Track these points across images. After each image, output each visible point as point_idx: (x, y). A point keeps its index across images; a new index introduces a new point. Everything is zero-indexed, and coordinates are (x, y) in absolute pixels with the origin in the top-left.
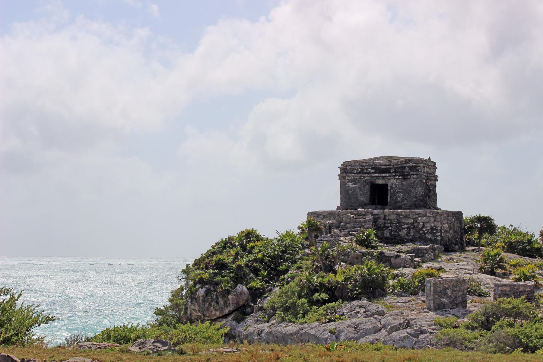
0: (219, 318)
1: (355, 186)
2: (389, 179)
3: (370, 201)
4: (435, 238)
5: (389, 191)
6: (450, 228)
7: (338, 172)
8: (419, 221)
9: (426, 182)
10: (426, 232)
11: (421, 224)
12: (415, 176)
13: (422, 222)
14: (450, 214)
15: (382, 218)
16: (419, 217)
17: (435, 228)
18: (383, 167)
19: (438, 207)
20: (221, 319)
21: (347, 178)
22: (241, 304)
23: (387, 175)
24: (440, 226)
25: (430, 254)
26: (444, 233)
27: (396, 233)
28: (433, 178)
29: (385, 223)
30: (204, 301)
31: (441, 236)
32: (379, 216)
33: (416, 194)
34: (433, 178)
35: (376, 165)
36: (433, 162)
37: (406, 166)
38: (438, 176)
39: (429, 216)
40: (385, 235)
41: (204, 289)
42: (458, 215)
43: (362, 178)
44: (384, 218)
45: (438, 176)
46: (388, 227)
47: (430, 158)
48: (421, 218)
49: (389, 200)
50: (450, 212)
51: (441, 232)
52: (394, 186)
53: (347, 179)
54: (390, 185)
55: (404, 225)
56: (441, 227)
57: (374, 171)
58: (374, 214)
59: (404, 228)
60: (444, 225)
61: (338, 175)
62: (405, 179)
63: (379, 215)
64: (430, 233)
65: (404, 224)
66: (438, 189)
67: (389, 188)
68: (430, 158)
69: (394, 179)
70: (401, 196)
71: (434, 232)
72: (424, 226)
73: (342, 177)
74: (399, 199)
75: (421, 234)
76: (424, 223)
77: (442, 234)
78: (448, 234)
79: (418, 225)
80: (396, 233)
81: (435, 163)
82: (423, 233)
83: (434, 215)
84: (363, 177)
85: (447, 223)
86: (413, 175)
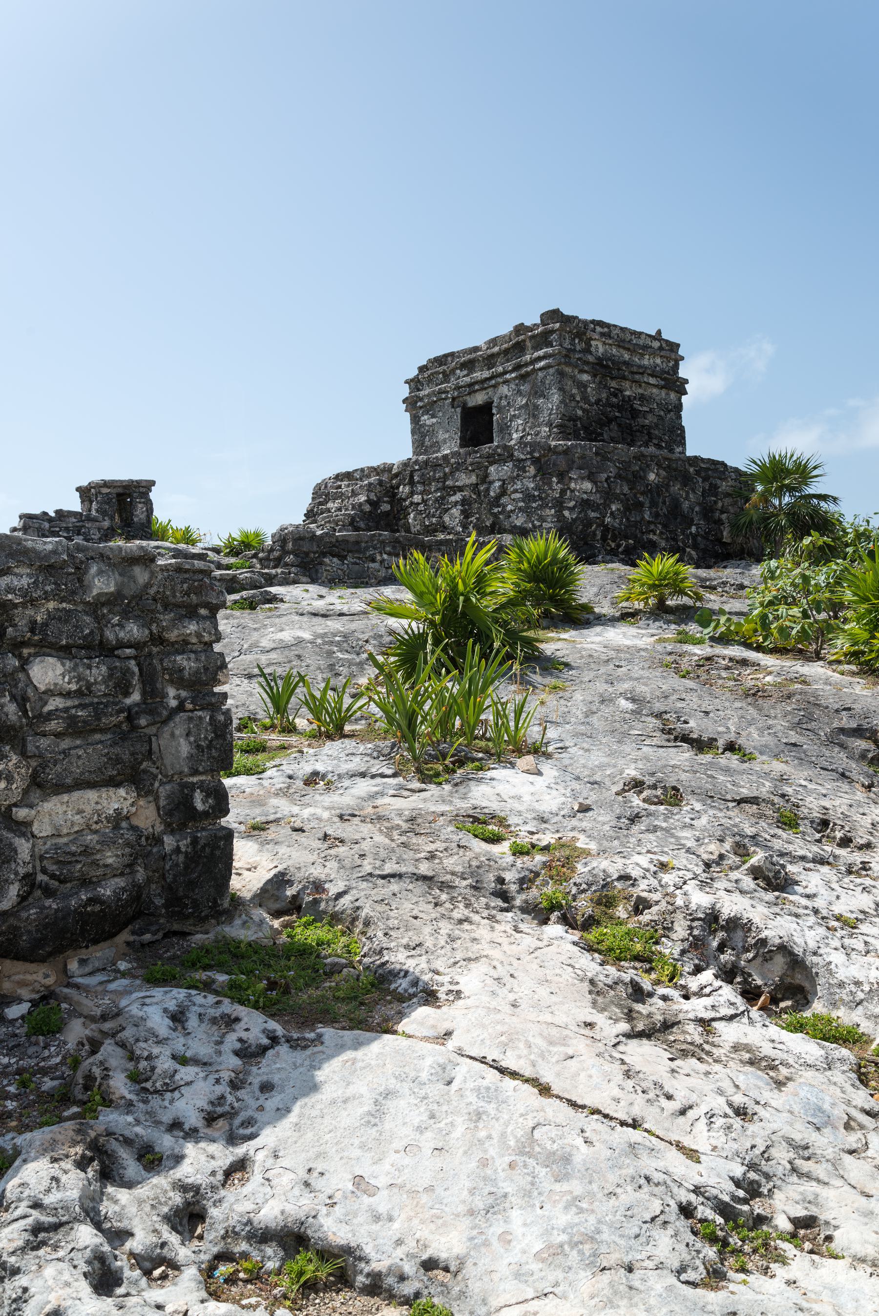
1: (434, 420)
4: (537, 523)
7: (405, 391)
8: (491, 478)
10: (509, 508)
11: (497, 484)
12: (542, 364)
13: (499, 480)
16: (491, 463)
17: (536, 493)
21: (419, 404)
24: (558, 487)
27: (434, 520)
29: (412, 493)
33: (550, 414)
37: (524, 341)
38: (686, 381)
39: (520, 461)
43: (443, 396)
46: (418, 504)
47: (659, 332)
48: (496, 466)
52: (504, 403)
53: (421, 407)
55: (455, 494)
56: (563, 492)
57: (465, 372)
59: (456, 503)
60: (573, 485)
61: (404, 401)
64: (520, 509)
67: (494, 411)
68: (659, 332)
69: (504, 382)
70: (520, 428)
71: (534, 505)
72: (503, 492)
73: (411, 403)
75: (495, 516)
76: (504, 481)
77: (566, 513)
79: (487, 490)
80: (434, 520)
81: (674, 347)
82: (500, 513)
83: (537, 455)
84: (444, 392)
86: (540, 359)
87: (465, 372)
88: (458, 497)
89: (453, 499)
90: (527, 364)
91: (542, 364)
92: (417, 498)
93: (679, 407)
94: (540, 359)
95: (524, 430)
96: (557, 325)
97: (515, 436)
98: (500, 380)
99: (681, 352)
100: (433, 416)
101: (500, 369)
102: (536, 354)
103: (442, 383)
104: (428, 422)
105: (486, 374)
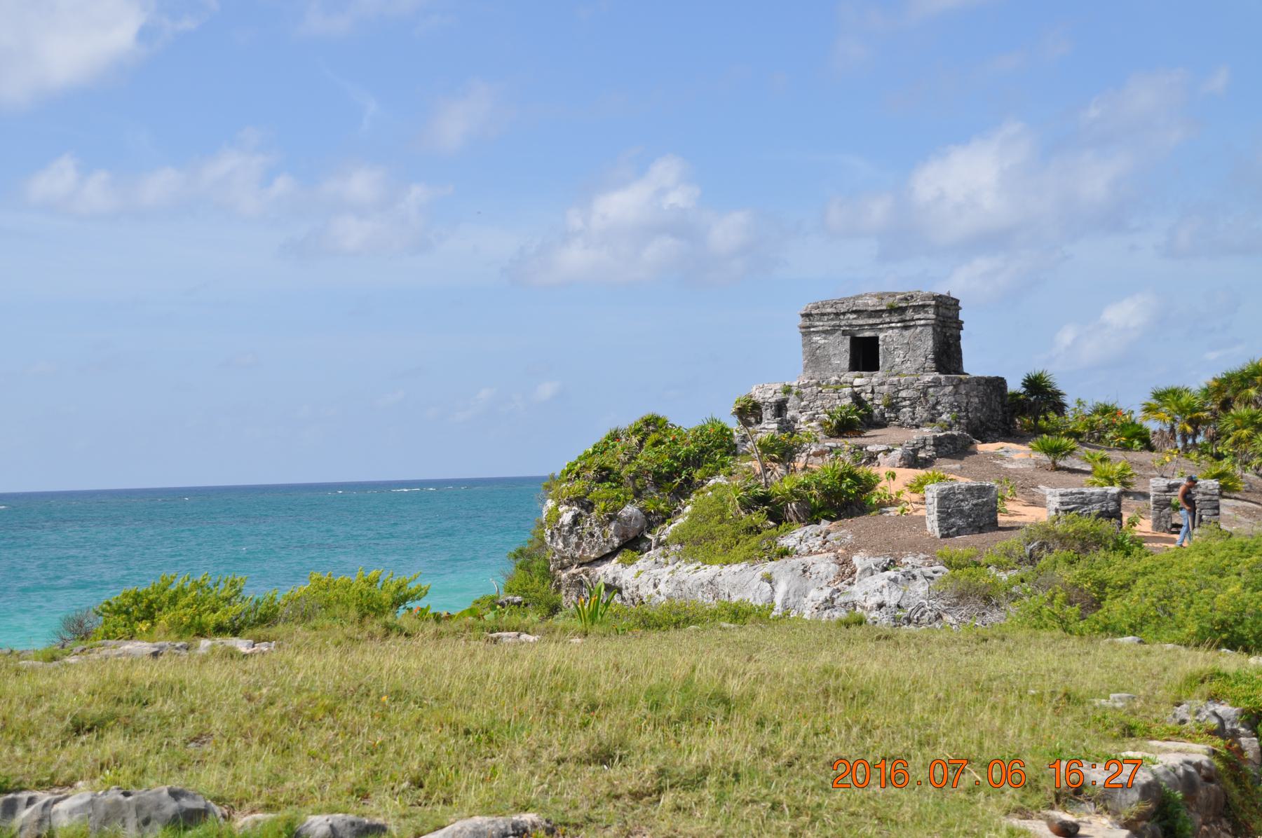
0: (596, 560)
1: (826, 341)
2: (880, 329)
3: (851, 364)
5: (881, 348)
6: (983, 403)
9: (941, 331)
12: (922, 322)
14: (983, 382)
15: (870, 391)
18: (870, 309)
19: (965, 371)
20: (599, 562)
22: (631, 536)
23: (878, 321)
25: (946, 446)
26: (972, 412)
28: (954, 325)
30: (571, 531)
31: (968, 418)
32: (863, 388)
34: (954, 325)
35: (859, 306)
36: (953, 299)
38: (962, 322)
40: (875, 419)
41: (571, 513)
42: (997, 384)
44: (873, 392)
45: (962, 322)
46: (879, 405)
49: (881, 363)
50: (982, 378)
51: (966, 410)
52: (888, 339)
54: (881, 336)
55: (905, 400)
56: (967, 404)
58: (855, 384)
60: (972, 400)
62: (906, 328)
63: (864, 386)
65: (905, 399)
66: (964, 344)
67: (880, 343)
68: (949, 293)
72: (938, 403)
74: (897, 360)
75: (933, 415)
78: (979, 415)
81: (957, 301)
85: (977, 396)
86: (920, 319)
87: (855, 316)
88: (908, 403)
89: (904, 404)
90: (909, 321)
91: (922, 322)
92: (877, 402)
93: (959, 338)
94: (920, 319)
95: (905, 357)
96: (933, 303)
97: (897, 360)
98: (885, 326)
99: (960, 305)
100: (825, 338)
101: (888, 320)
102: (916, 316)
103: (832, 320)
104: (820, 342)
105: (878, 321)
